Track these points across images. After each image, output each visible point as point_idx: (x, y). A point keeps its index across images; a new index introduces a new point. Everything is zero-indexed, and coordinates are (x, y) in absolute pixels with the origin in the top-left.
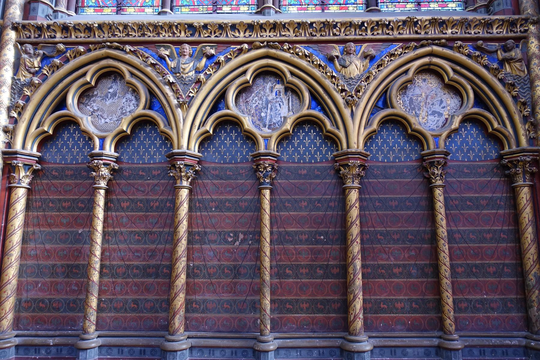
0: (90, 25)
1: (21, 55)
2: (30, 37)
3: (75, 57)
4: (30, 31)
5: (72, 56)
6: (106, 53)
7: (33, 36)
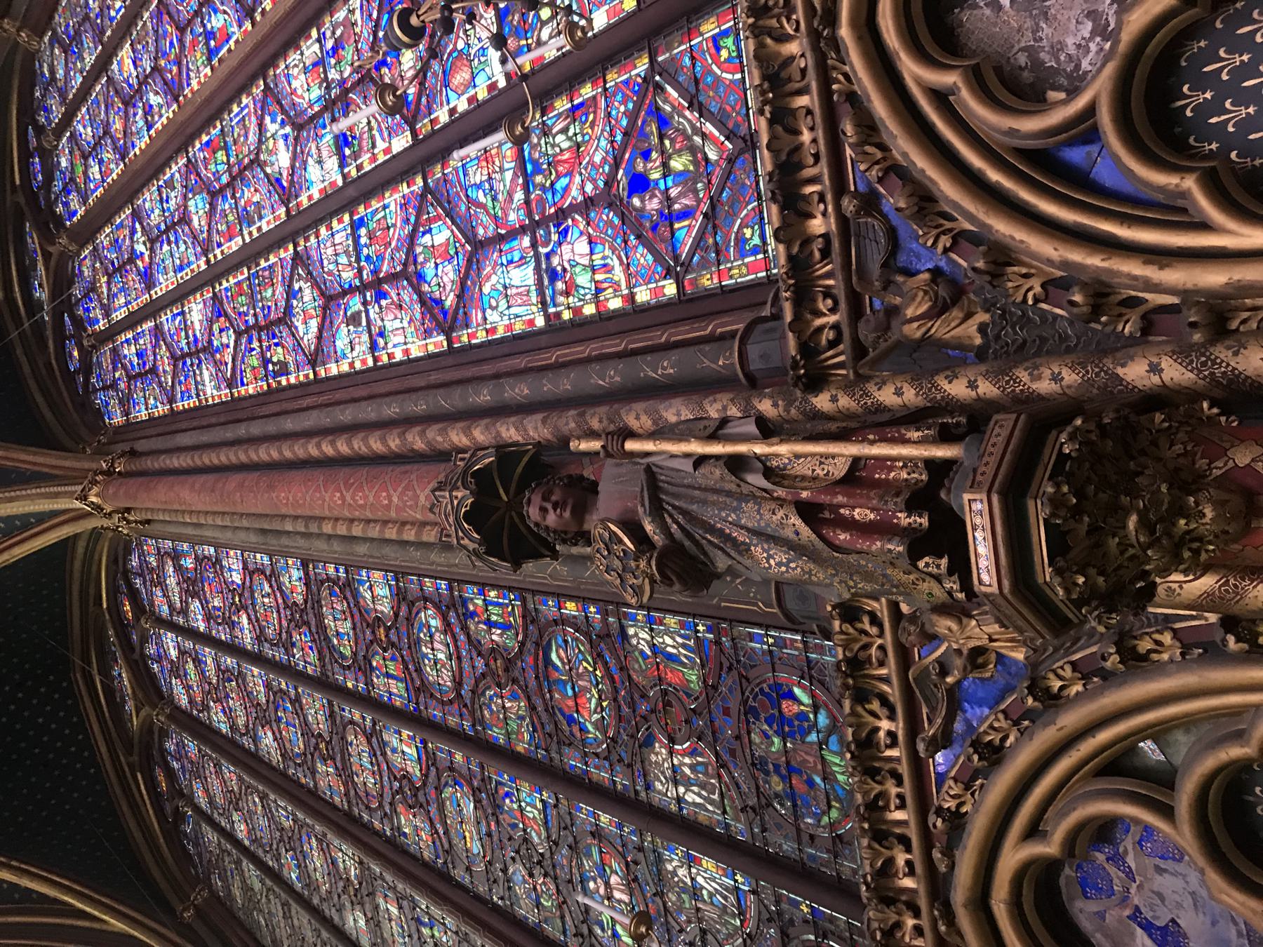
0: (765, 103)
1: (898, 344)
2: (836, 327)
3: (883, 147)
5: (879, 155)
6: (854, 24)
7: (832, 319)
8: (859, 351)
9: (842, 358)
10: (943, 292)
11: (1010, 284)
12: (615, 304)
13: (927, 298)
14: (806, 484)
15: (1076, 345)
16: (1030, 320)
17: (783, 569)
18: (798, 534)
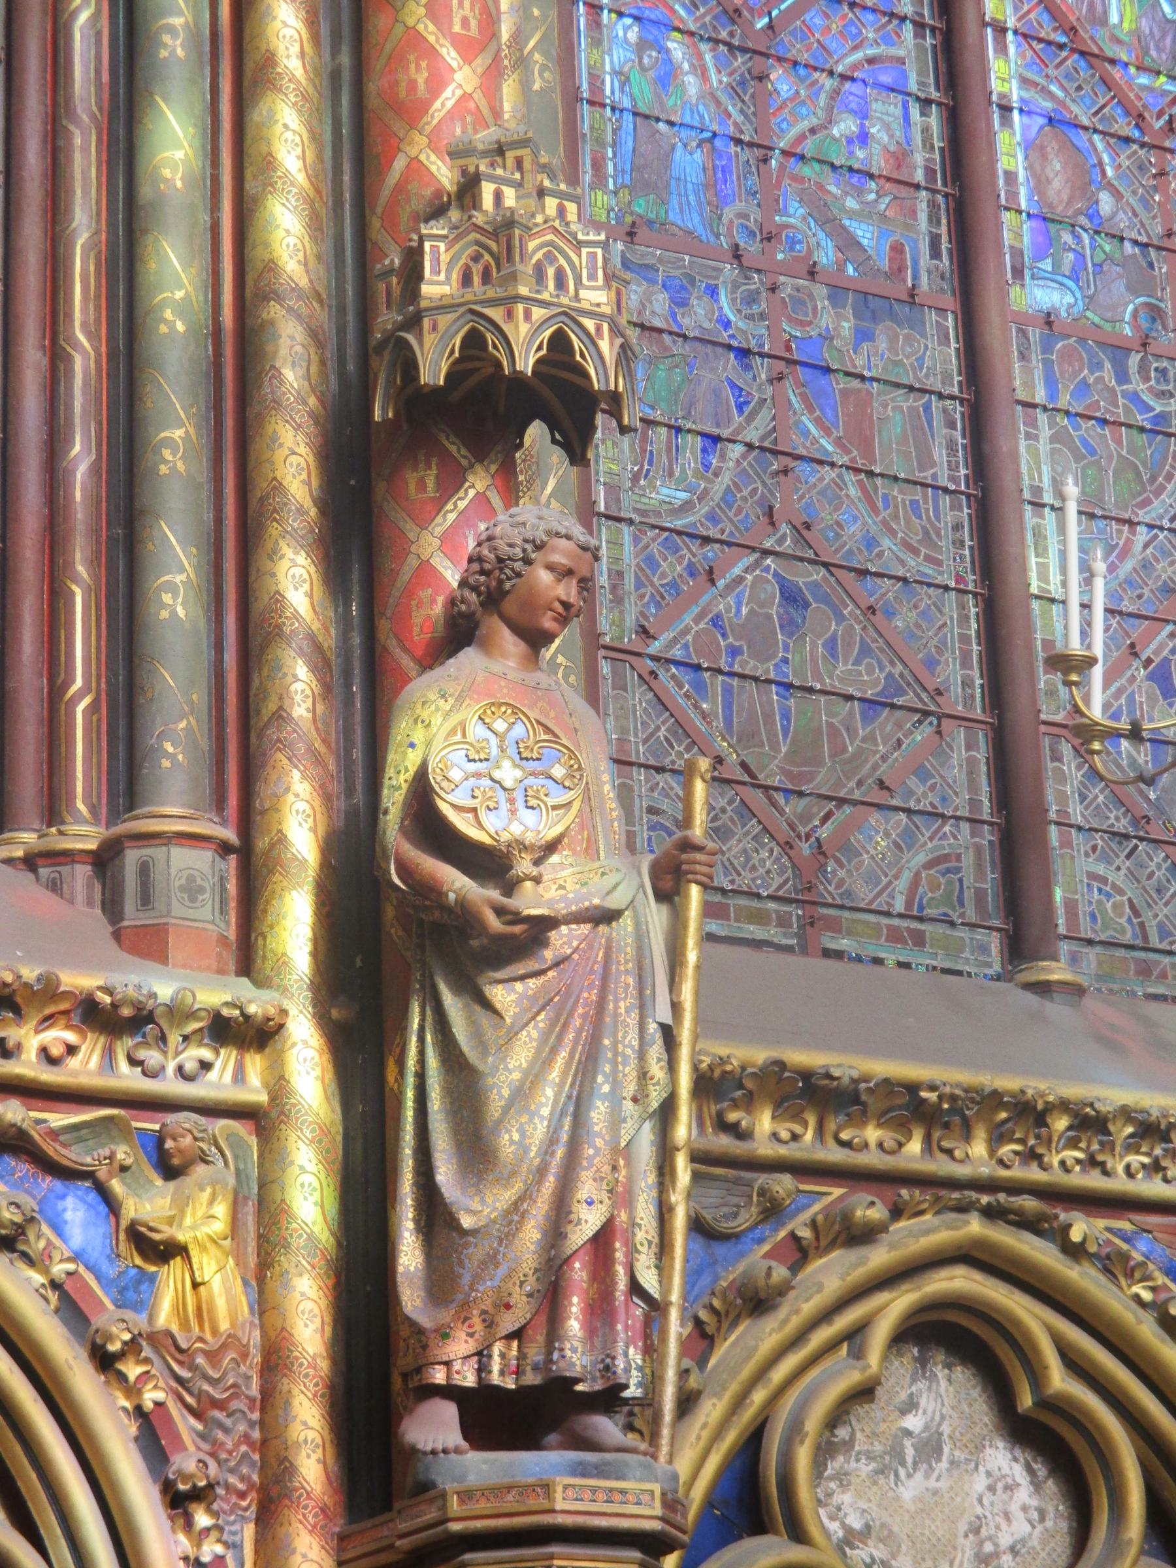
17: (516, 1137)
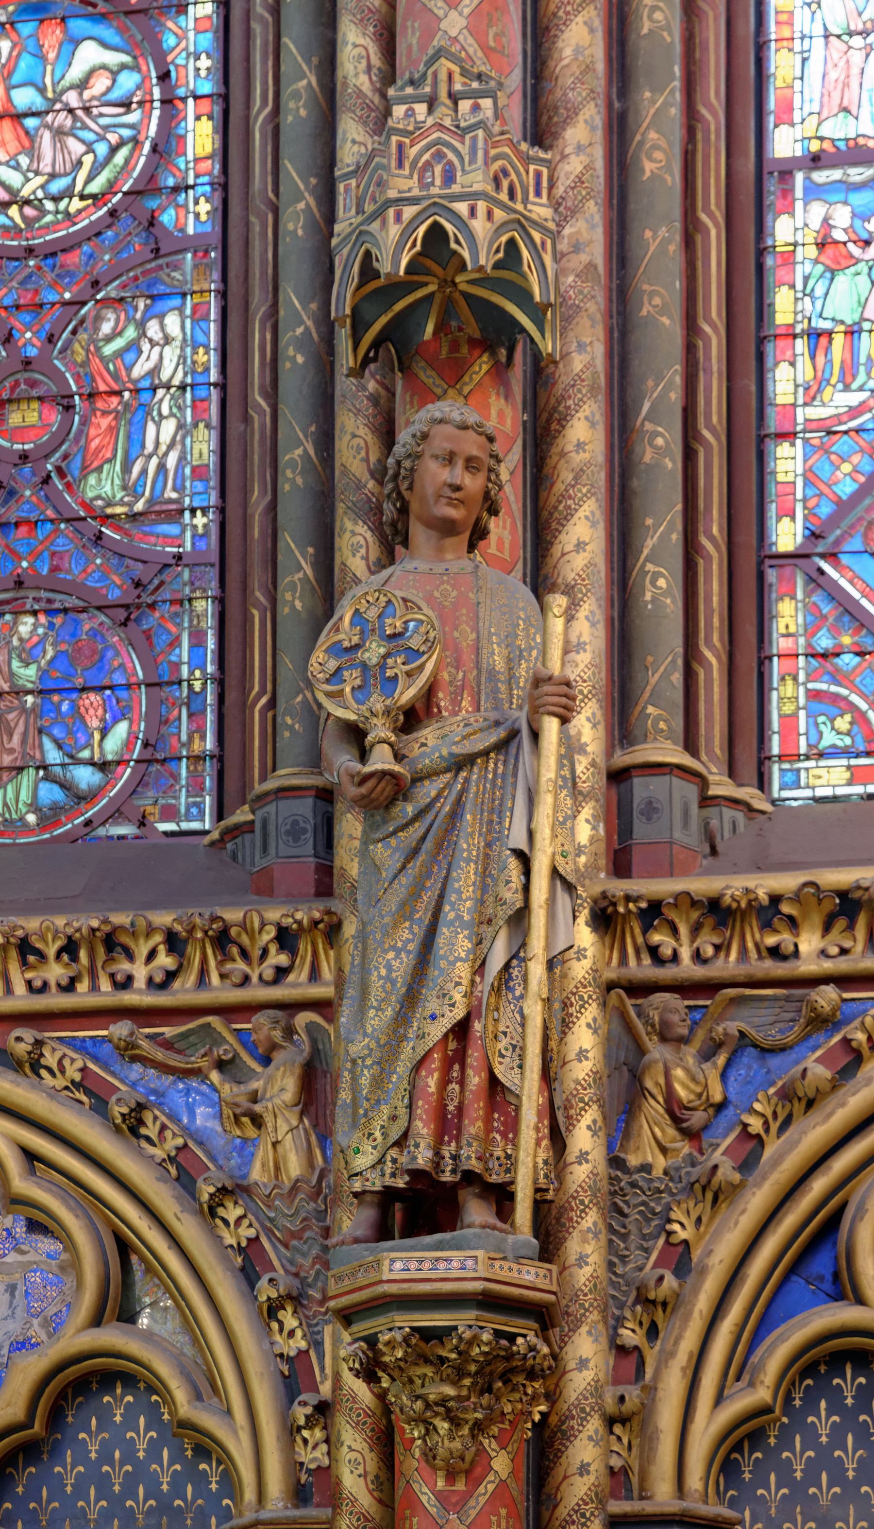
1: (641, 1051)
2: (675, 957)
4: (674, 931)
7: (685, 953)
8: (640, 989)
9: (632, 961)
10: (697, 1119)
11: (691, 1204)
12: (784, 382)
13: (692, 1097)
14: (491, 1028)
15: (615, 1273)
16: (648, 1220)
17: (383, 972)
18: (433, 1017)
